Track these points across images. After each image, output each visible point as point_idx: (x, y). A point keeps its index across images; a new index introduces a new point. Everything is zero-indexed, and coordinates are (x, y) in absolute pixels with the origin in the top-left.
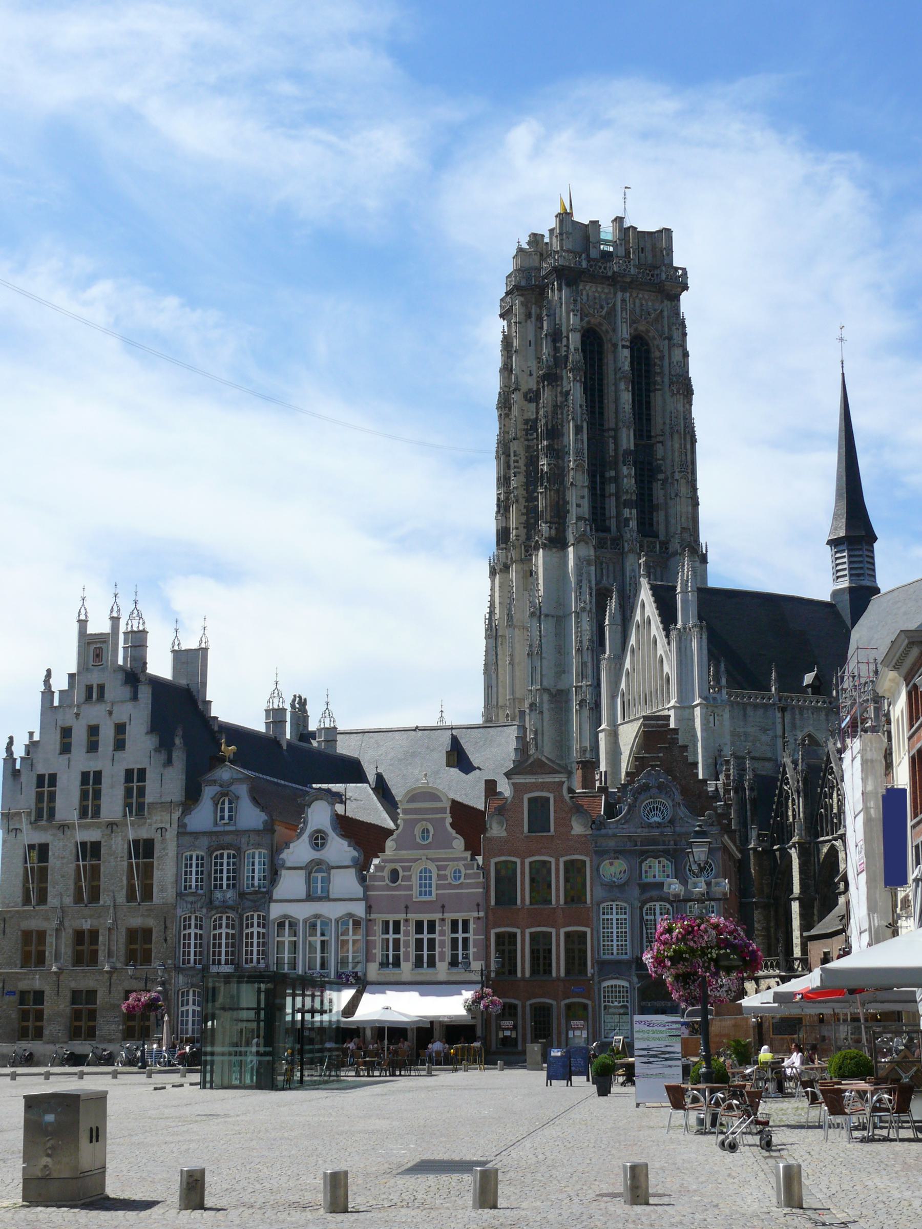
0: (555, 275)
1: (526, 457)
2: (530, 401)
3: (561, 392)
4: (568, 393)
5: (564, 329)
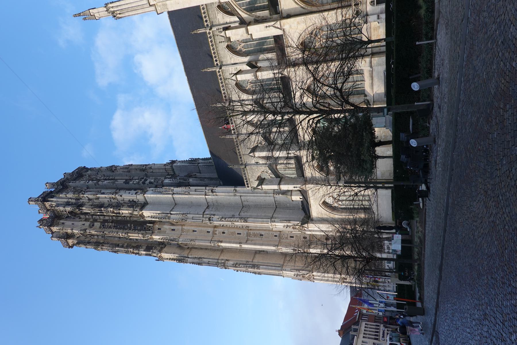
0: (46, 203)
1: (113, 229)
2: (93, 225)
3: (88, 203)
4: (89, 199)
5: (66, 200)
